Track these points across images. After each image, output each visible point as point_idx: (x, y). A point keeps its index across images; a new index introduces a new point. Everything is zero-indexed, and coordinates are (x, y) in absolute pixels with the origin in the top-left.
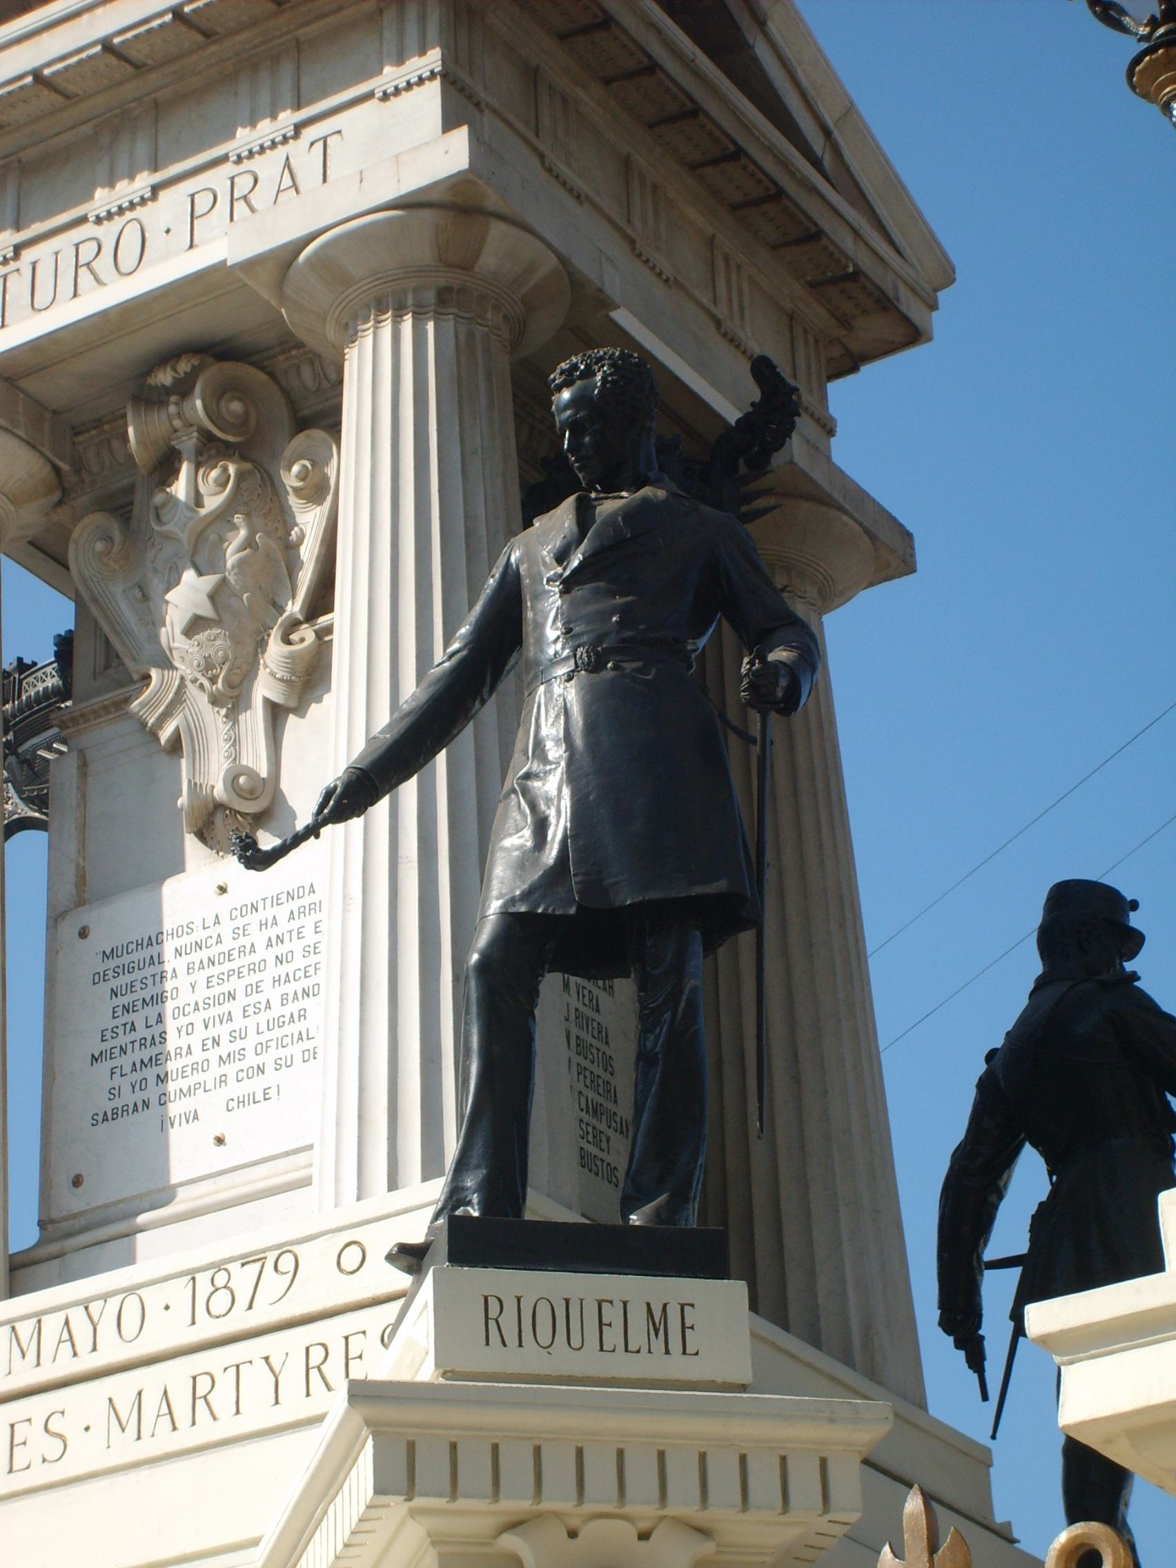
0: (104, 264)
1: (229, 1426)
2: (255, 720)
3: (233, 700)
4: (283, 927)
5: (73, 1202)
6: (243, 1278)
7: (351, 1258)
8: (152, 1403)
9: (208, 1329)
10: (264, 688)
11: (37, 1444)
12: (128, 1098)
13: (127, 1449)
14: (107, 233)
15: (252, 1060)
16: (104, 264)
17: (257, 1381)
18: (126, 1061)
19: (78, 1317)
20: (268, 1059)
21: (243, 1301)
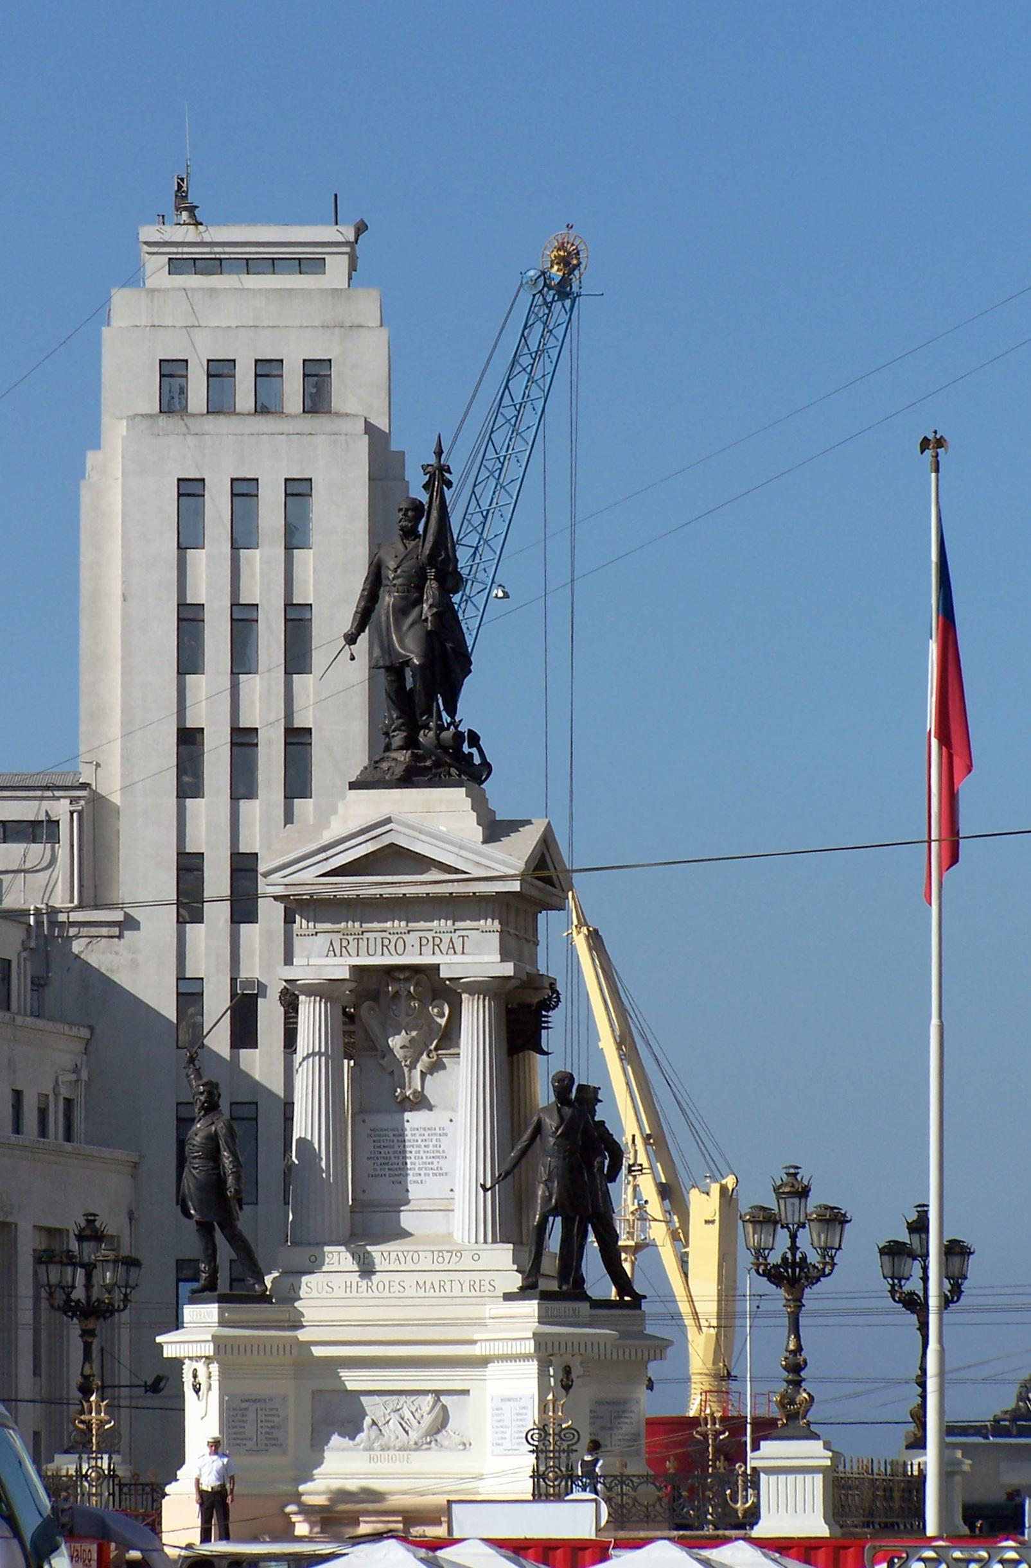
0: (392, 948)
1: (448, 1294)
2: (417, 1073)
3: (412, 1066)
4: (426, 1137)
6: (447, 1256)
7: (476, 1257)
8: (428, 1285)
9: (436, 1267)
10: (419, 1067)
11: (396, 1287)
12: (379, 1172)
13: (421, 1293)
14: (394, 938)
15: (417, 1171)
16: (392, 948)
17: (456, 1285)
18: (379, 1162)
19: (400, 1254)
20: (422, 1172)
21: (447, 1260)
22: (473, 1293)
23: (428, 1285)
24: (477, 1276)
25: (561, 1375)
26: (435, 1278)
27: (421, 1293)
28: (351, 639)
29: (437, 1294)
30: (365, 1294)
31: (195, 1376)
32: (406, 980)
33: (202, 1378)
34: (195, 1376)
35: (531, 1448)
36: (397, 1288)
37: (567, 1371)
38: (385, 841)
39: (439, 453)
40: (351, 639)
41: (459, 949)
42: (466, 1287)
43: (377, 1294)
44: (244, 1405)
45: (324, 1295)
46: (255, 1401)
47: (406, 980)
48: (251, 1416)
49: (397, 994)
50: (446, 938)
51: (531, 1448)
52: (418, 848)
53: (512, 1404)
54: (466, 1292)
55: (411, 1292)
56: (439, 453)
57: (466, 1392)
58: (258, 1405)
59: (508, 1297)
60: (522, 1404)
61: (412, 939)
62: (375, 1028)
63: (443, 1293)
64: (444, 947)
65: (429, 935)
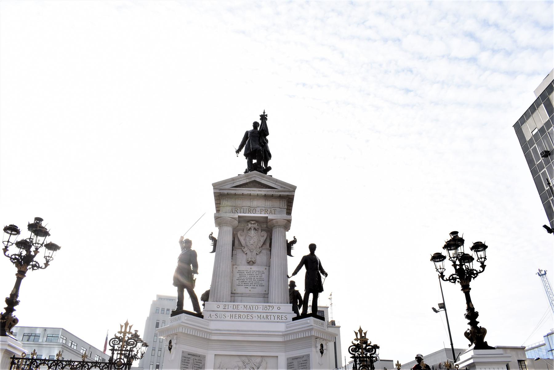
1: (269, 320)
5: (234, 292)
6: (268, 308)
17: (272, 317)
22: (279, 320)
23: (262, 316)
24: (280, 315)
25: (319, 347)
26: (265, 315)
27: (259, 320)
28: (238, 151)
29: (265, 320)
30: (238, 319)
32: (254, 224)
33: (173, 344)
34: (170, 342)
35: (352, 356)
36: (250, 317)
37: (322, 346)
38: (253, 179)
39: (264, 113)
40: (238, 151)
41: (273, 213)
42: (276, 318)
43: (242, 319)
44: (189, 356)
45: (222, 319)
46: (194, 355)
47: (254, 224)
48: (191, 361)
49: (250, 228)
50: (269, 210)
51: (352, 356)
52: (263, 182)
53: (299, 360)
54: (276, 320)
55: (255, 319)
56: (264, 113)
57: (277, 357)
58: (194, 357)
59: (294, 319)
60: (304, 359)
61: (258, 209)
62: (242, 239)
63: (267, 320)
64: (268, 212)
65: (264, 209)
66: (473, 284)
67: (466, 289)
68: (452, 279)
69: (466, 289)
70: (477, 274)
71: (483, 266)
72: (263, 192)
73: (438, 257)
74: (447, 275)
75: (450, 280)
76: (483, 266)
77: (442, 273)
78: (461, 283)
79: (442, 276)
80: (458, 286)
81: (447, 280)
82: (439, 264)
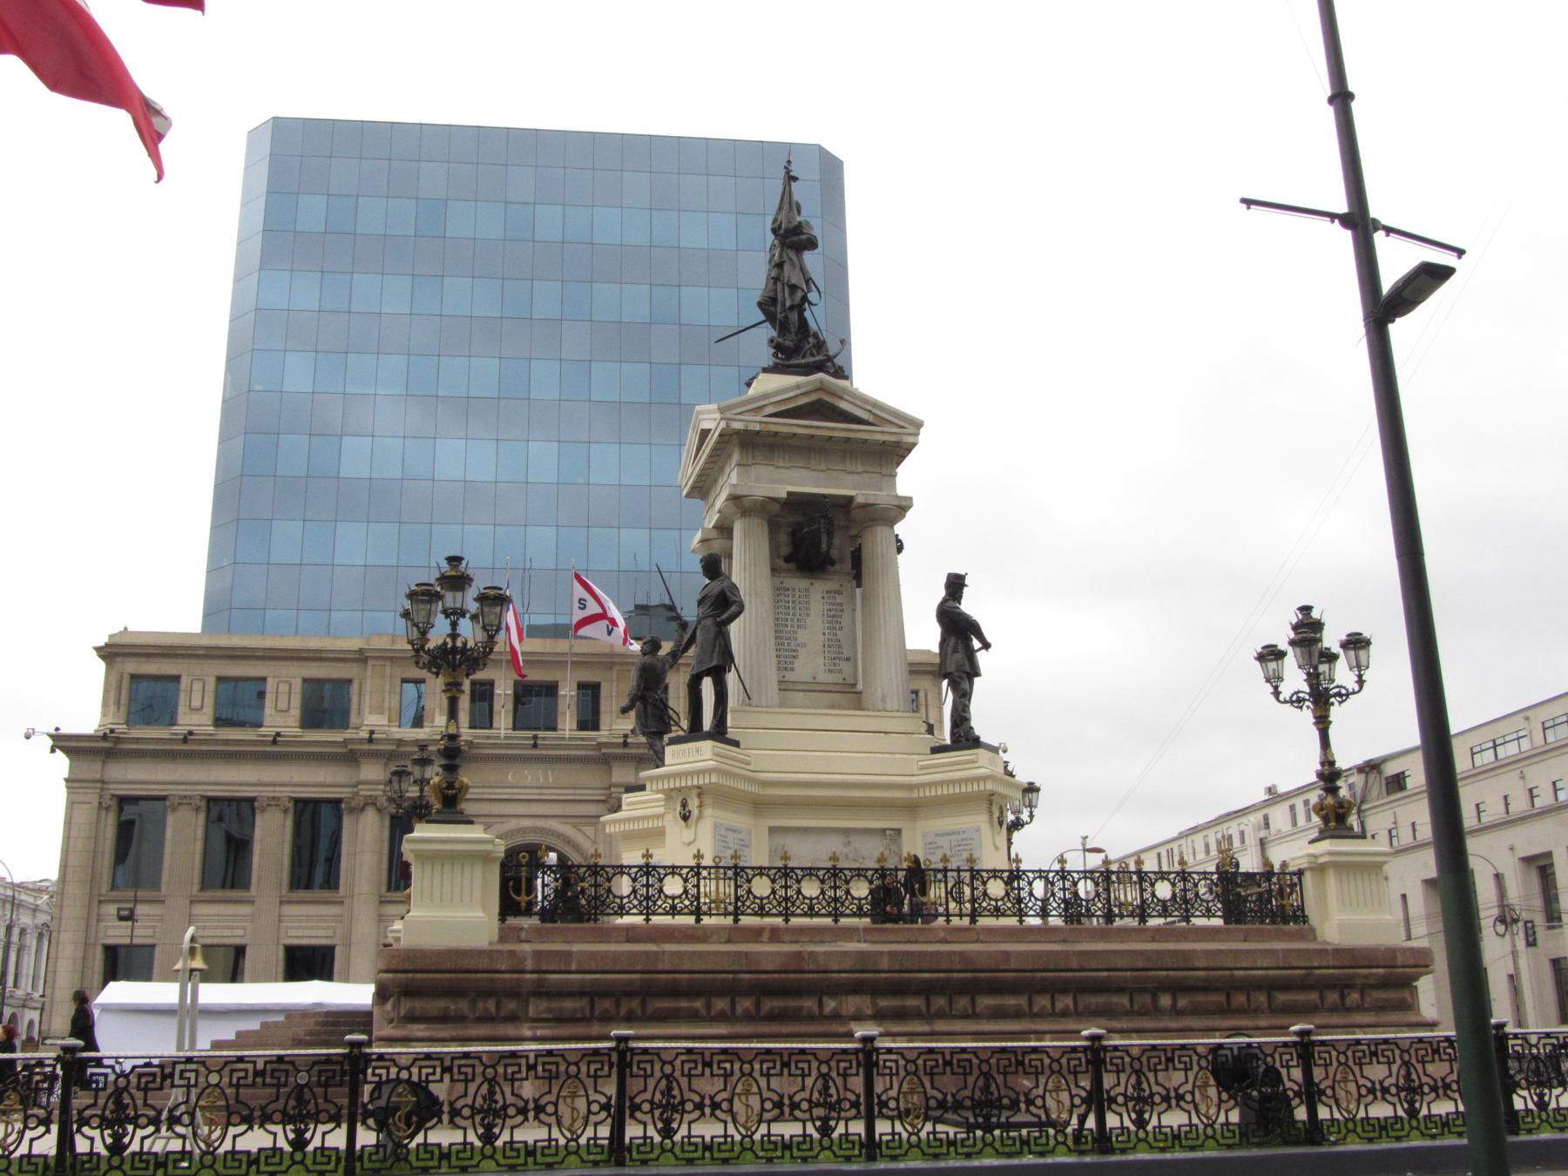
31: (684, 805)
34: (684, 805)
66: (1336, 712)
67: (1323, 723)
68: (1297, 701)
69: (1323, 723)
70: (1347, 695)
71: (1361, 682)
72: (837, 429)
73: (1271, 655)
74: (1286, 690)
75: (1291, 702)
76: (1361, 682)
77: (1276, 688)
78: (1314, 711)
79: (1276, 693)
80: (1307, 716)
81: (1285, 702)
82: (1272, 665)
